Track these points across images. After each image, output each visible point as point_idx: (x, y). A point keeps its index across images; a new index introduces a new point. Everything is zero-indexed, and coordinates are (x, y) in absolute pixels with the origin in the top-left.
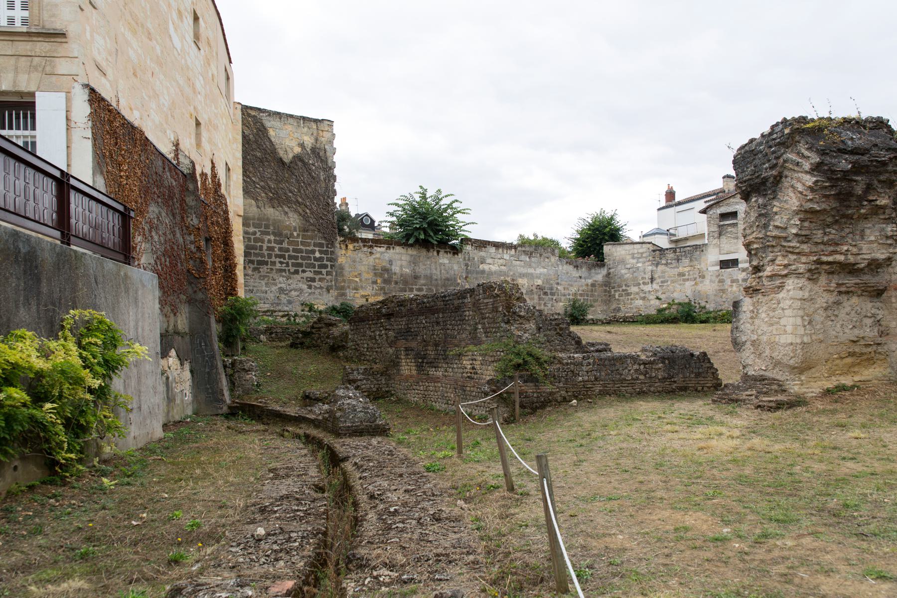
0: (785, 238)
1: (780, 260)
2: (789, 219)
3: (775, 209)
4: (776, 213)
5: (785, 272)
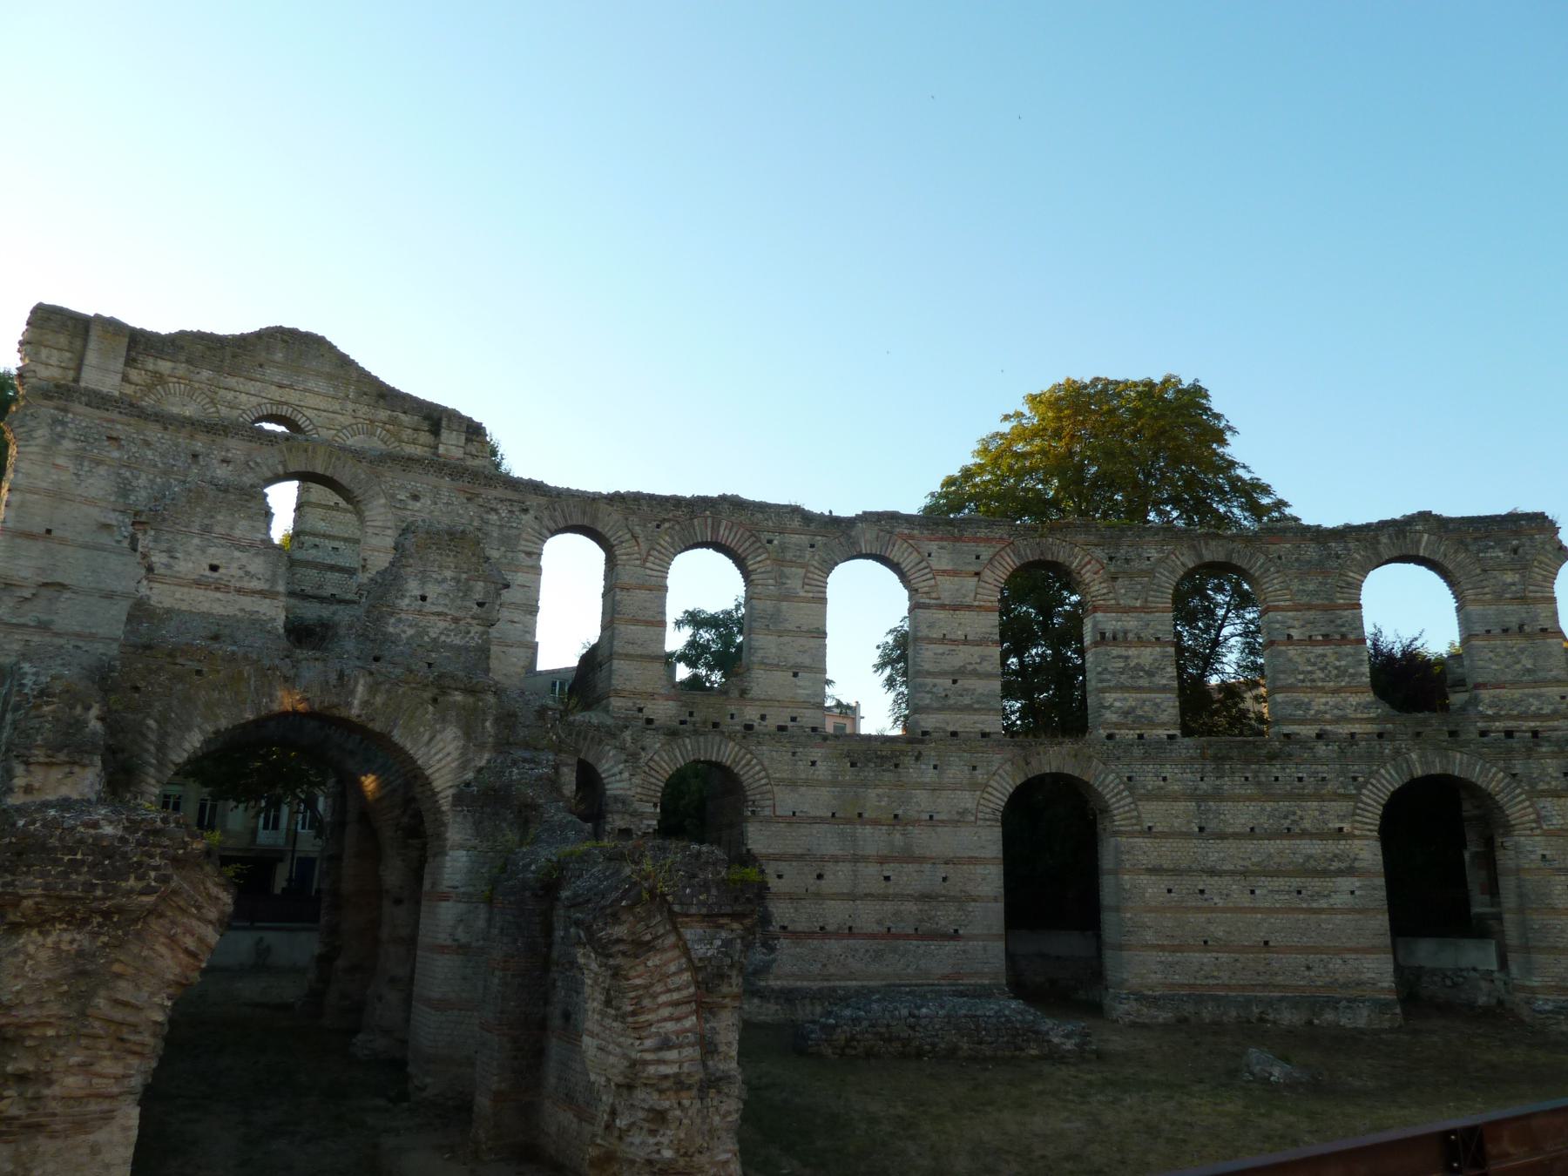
0: (134, 1028)
1: (108, 1066)
2: (152, 994)
3: (117, 968)
4: (119, 976)
5: (115, 1090)
